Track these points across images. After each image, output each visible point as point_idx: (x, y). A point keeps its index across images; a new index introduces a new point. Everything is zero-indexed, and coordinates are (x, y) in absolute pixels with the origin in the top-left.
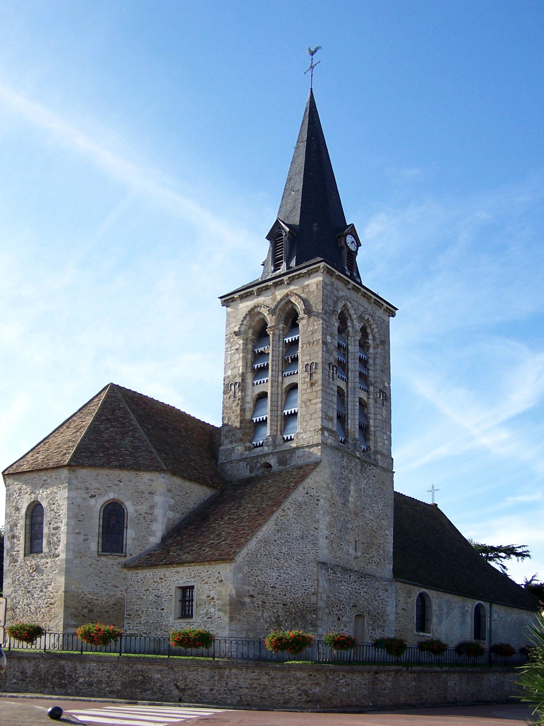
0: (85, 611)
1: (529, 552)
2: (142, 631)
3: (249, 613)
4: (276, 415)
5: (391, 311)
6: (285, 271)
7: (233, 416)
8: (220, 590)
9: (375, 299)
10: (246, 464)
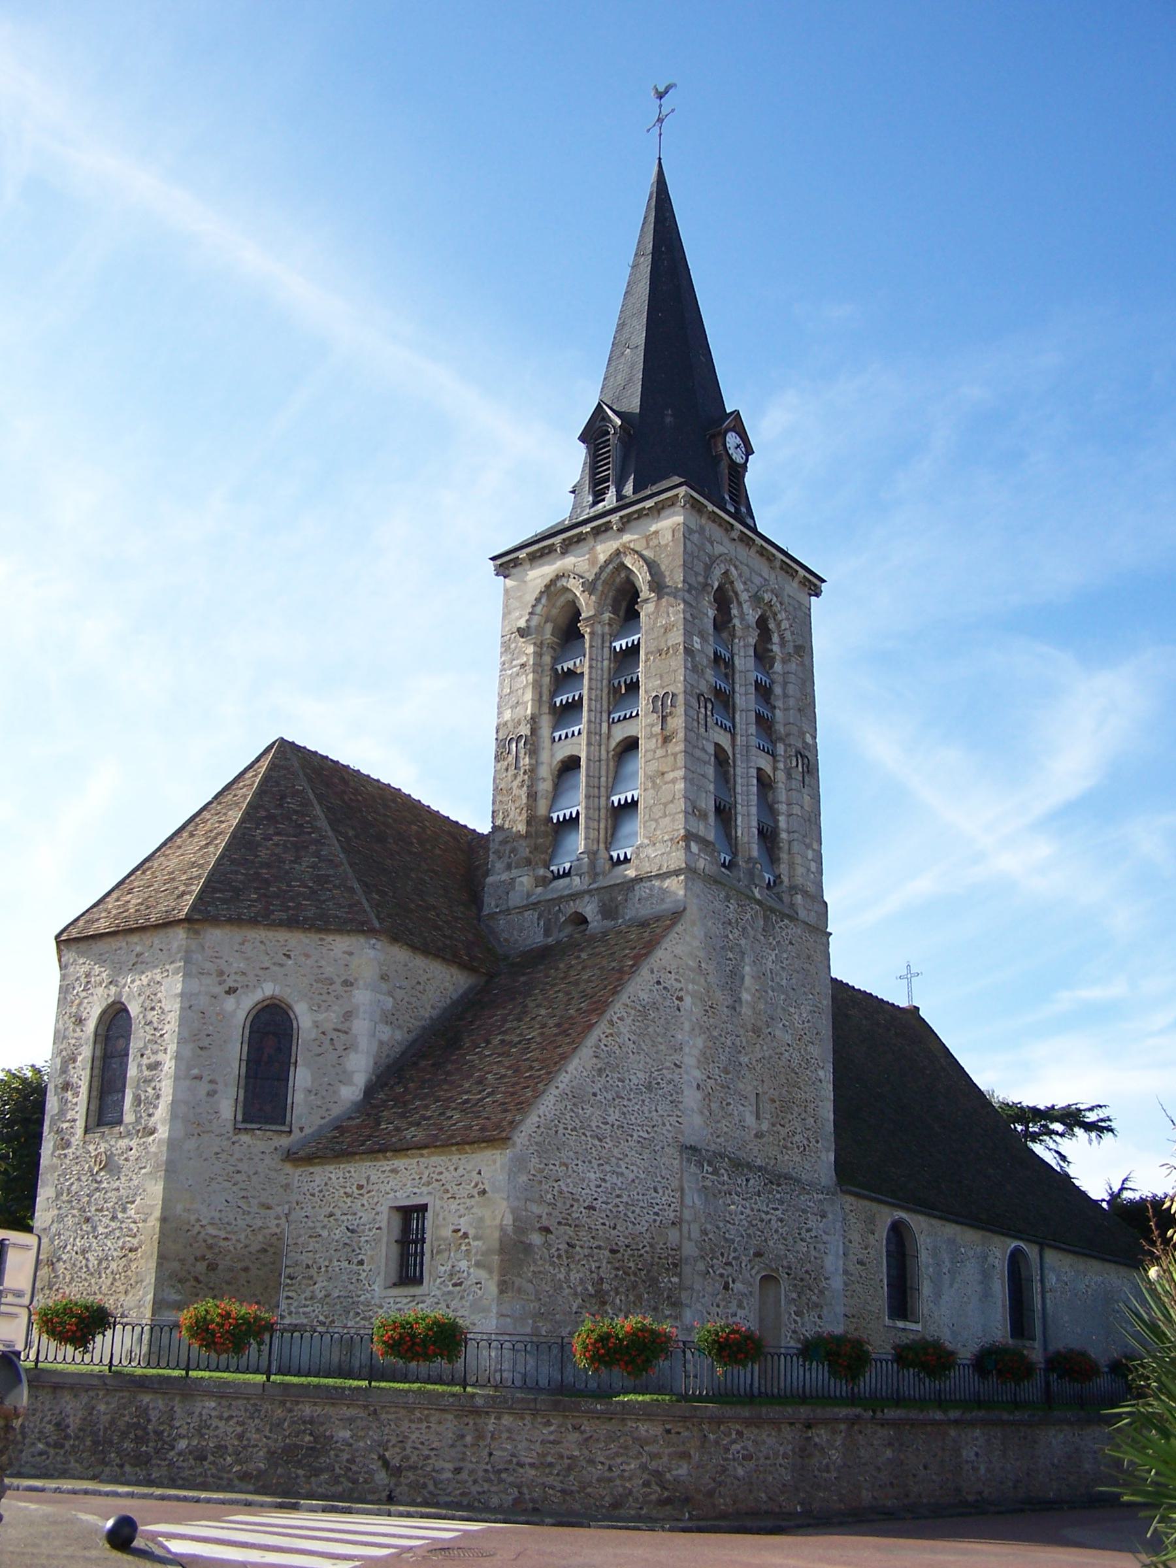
0: (201, 1267)
1: (1110, 1120)
2: (317, 1317)
3: (540, 1272)
4: (596, 807)
5: (813, 584)
6: (614, 504)
7: (513, 808)
8: (480, 1215)
9: (782, 560)
10: (536, 916)
